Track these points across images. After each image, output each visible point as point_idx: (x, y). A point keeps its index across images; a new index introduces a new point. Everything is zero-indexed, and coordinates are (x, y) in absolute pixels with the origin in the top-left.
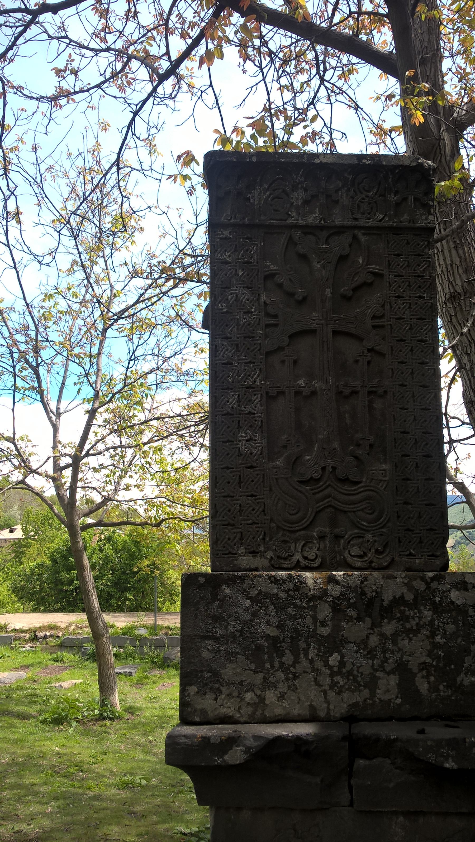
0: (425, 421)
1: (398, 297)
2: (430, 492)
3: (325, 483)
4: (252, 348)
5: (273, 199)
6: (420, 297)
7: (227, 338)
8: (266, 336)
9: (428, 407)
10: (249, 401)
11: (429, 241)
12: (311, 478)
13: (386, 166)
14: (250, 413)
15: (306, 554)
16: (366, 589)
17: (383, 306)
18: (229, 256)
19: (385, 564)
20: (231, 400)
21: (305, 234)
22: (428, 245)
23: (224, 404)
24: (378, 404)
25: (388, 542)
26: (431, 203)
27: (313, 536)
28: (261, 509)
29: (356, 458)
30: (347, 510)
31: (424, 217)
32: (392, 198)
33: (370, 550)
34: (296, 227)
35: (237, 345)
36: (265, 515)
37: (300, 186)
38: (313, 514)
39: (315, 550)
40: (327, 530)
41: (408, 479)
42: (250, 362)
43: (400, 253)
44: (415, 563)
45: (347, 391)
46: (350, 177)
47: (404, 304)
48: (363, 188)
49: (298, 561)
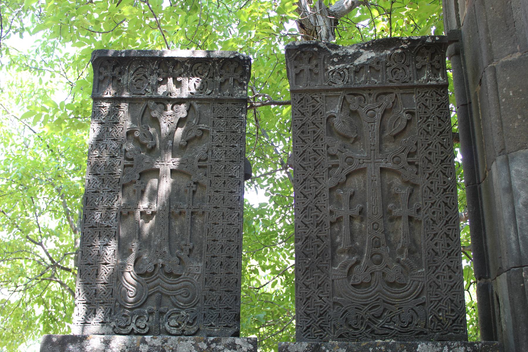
0: (230, 233)
1: (218, 146)
2: (229, 282)
3: (156, 275)
4: (113, 181)
5: (136, 81)
6: (233, 146)
7: (97, 175)
8: (124, 174)
9: (233, 223)
10: (108, 218)
11: (242, 108)
12: (147, 272)
13: (213, 58)
14: (108, 226)
15: (138, 324)
16: (165, 348)
17: (207, 152)
18: (104, 119)
19: (193, 332)
20: (96, 217)
21: (157, 103)
22: (242, 111)
23: (91, 220)
24: (199, 220)
25: (196, 317)
26: (245, 82)
27: (144, 312)
28: (110, 293)
29: (180, 258)
30: (169, 294)
31: (240, 92)
32: (218, 79)
33: (184, 322)
34: (151, 99)
35: (103, 180)
36: (112, 297)
37: (155, 72)
38: (146, 297)
39: (145, 322)
40: (155, 308)
41: (214, 273)
42: (111, 191)
43: (221, 116)
44: (214, 331)
45: (178, 211)
46: (189, 66)
47: (221, 150)
48: (199, 73)
49: (133, 329)
